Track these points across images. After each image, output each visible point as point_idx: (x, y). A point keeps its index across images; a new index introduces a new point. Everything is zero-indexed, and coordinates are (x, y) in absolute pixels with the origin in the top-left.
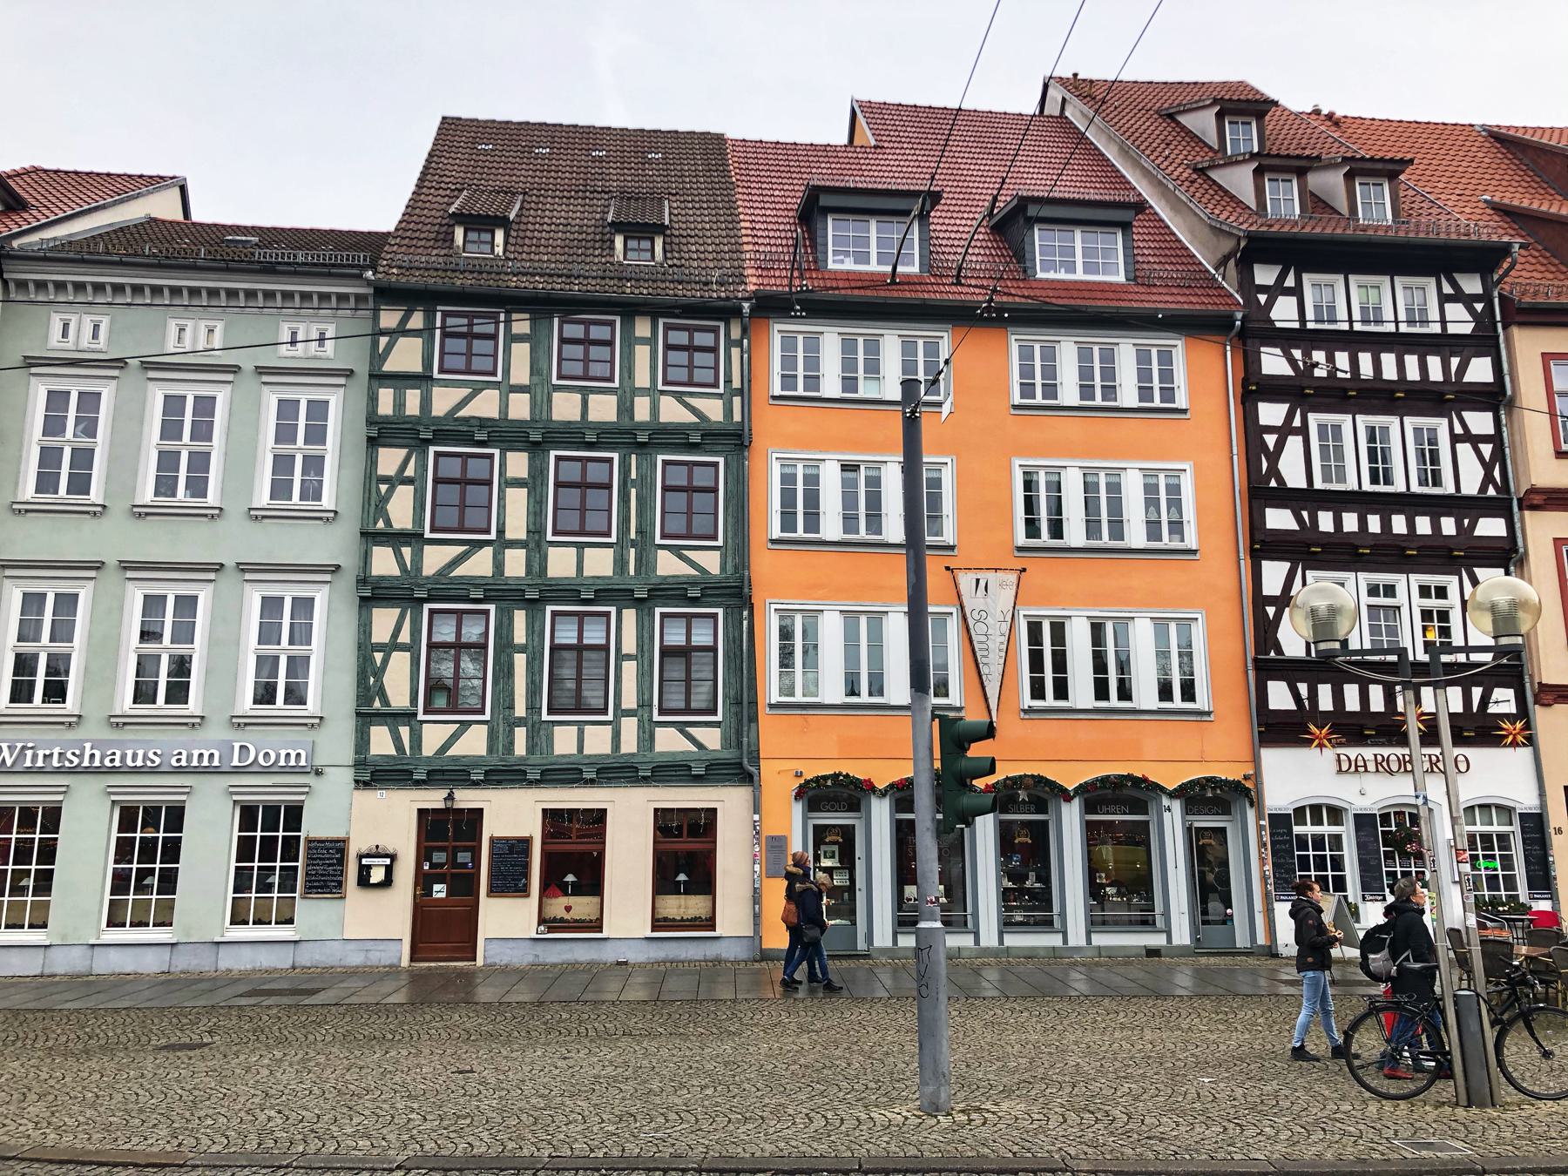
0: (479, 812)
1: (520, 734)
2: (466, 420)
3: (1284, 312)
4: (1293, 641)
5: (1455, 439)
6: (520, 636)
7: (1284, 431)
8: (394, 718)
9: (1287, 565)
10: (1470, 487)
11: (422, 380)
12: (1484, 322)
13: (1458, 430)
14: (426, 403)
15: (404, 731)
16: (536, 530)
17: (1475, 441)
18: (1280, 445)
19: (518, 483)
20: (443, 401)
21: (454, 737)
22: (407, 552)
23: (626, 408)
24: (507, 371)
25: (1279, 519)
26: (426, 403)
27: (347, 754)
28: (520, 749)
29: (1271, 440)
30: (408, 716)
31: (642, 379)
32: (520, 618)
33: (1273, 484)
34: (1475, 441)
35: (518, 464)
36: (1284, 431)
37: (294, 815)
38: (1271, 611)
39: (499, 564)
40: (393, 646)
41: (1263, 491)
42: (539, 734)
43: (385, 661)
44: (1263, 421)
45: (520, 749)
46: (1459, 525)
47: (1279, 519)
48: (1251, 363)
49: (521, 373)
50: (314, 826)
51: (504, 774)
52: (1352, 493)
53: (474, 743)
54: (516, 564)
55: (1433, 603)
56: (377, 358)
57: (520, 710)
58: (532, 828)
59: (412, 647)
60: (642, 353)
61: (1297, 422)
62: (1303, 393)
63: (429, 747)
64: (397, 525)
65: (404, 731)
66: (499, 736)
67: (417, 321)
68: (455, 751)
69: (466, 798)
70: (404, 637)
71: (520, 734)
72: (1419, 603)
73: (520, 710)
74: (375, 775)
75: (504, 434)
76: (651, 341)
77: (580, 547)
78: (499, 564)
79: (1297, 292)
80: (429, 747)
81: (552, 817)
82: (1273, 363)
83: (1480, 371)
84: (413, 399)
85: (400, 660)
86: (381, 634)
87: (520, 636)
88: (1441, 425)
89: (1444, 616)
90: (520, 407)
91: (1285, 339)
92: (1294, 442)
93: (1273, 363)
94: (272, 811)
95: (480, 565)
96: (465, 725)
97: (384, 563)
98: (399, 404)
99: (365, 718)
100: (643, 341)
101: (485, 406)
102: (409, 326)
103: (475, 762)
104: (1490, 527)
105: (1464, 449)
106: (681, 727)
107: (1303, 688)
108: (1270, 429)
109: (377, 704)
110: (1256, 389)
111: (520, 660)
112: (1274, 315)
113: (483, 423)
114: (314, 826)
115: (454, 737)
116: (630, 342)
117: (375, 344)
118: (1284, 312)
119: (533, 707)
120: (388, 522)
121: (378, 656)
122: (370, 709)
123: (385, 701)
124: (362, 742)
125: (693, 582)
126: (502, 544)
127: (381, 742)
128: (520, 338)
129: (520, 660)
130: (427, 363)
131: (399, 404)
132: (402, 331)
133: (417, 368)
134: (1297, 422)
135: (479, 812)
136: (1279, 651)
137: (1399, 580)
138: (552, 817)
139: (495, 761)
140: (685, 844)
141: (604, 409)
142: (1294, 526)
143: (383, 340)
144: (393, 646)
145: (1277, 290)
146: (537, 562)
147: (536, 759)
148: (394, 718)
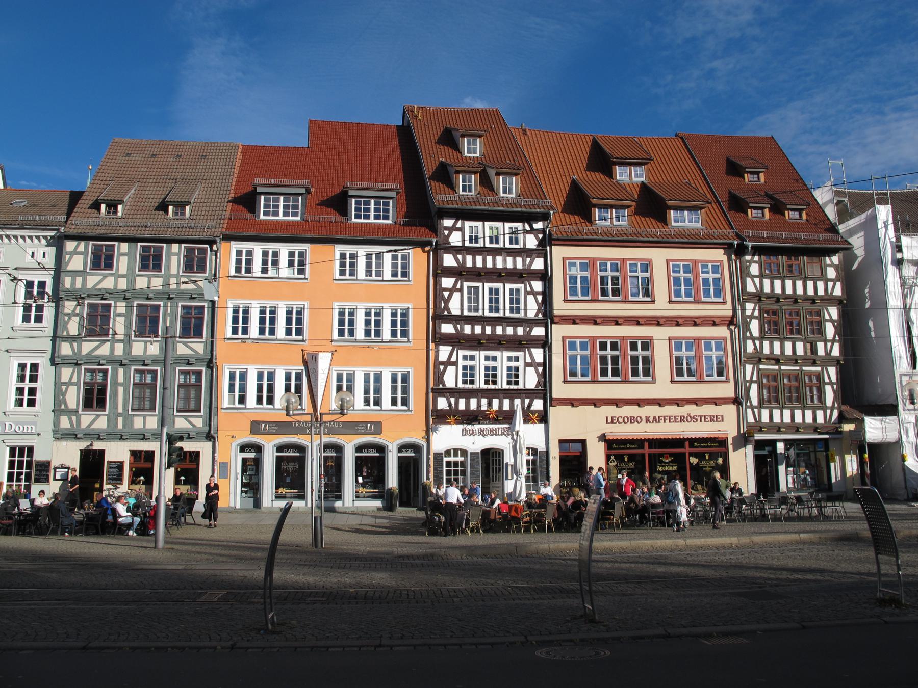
0: (102, 452)
1: (120, 420)
2: (100, 290)
3: (455, 239)
4: (450, 379)
5: (527, 293)
6: (121, 379)
7: (452, 290)
8: (71, 413)
9: (450, 348)
10: (531, 314)
11: (82, 273)
12: (542, 244)
13: (529, 289)
14: (84, 282)
15: (74, 418)
16: (128, 336)
17: (534, 294)
18: (450, 296)
19: (121, 315)
20: (91, 281)
22: (75, 345)
23: (166, 284)
24: (118, 269)
25: (447, 328)
26: (84, 282)
27: (50, 427)
29: (446, 294)
30: (75, 412)
31: (174, 271)
32: (121, 371)
33: (446, 313)
34: (534, 294)
35: (121, 308)
36: (452, 290)
37: (31, 450)
38: (442, 367)
39: (112, 349)
40: (69, 383)
41: (439, 316)
42: (128, 420)
43: (67, 390)
44: (444, 286)
45: (120, 426)
46: (525, 330)
47: (447, 328)
48: (438, 261)
49: (123, 270)
50: (38, 457)
52: (480, 317)
53: (102, 423)
54: (119, 349)
55: (513, 364)
57: (120, 410)
58: (126, 459)
59: (77, 384)
60: (174, 259)
61: (458, 286)
62: (459, 273)
63: (84, 425)
64: (72, 333)
65: (74, 418)
66: (112, 421)
68: (94, 426)
69: (98, 446)
70: (74, 380)
71: (120, 420)
72: (507, 364)
73: (120, 410)
74: (61, 435)
75: (116, 294)
76: (178, 254)
77: (146, 342)
78: (112, 349)
79: (461, 230)
80: (84, 425)
81: (134, 454)
82: (449, 260)
83: (538, 264)
84: (79, 280)
85: (72, 390)
86: (65, 378)
87: (121, 379)
88: (520, 286)
89: (517, 369)
90: (123, 284)
91: (455, 250)
92: (457, 295)
93: (449, 260)
94: (22, 450)
95: (105, 350)
96: (98, 416)
97: (66, 349)
98: (73, 283)
100: (175, 254)
101: (108, 284)
102: (78, 250)
103: (103, 430)
104: (539, 331)
105: (530, 298)
106: (186, 418)
107: (453, 400)
108: (446, 289)
109: (63, 407)
110: (440, 271)
111: (121, 390)
112: (451, 240)
113: (107, 291)
114: (38, 457)
116: (169, 254)
118: (455, 239)
119: (125, 408)
120: (68, 332)
121: (64, 388)
122: (59, 410)
124: (57, 422)
125: (192, 356)
126: (114, 341)
127: (65, 423)
128: (124, 254)
129: (121, 390)
131: (73, 283)
132: (75, 252)
134: (458, 286)
135: (102, 452)
136: (444, 385)
137: (497, 353)
138: (134, 454)
139: (111, 431)
140: (143, 465)
141: (157, 283)
142: (453, 331)
144: (69, 383)
145: (453, 229)
146: (128, 349)
147: (126, 430)
148: (71, 413)
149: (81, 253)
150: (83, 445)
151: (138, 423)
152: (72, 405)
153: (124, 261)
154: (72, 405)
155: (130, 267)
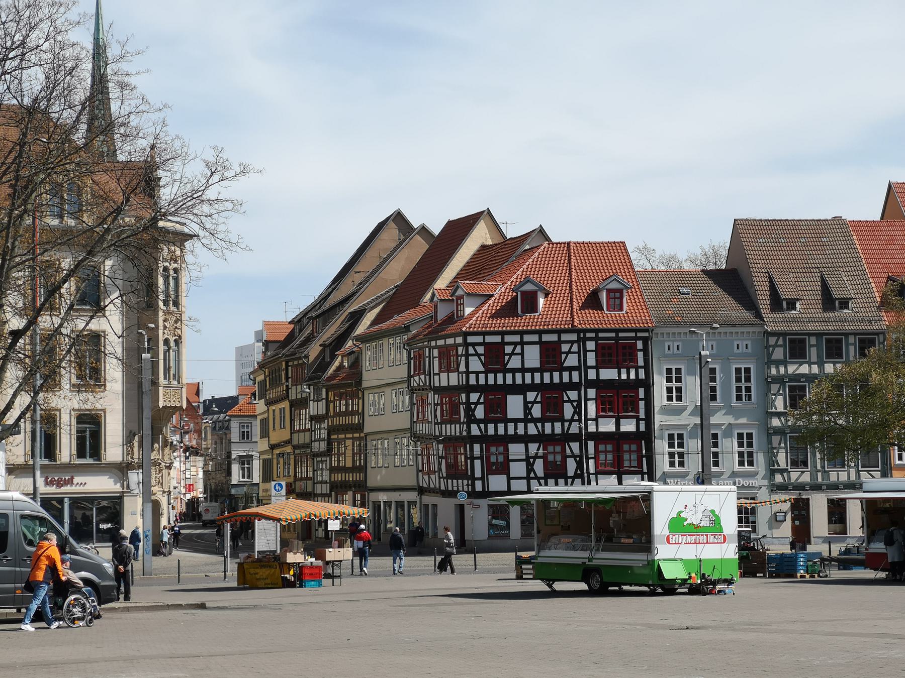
8: (782, 471)
15: (785, 474)
20: (791, 369)
21: (800, 476)
28: (820, 480)
30: (786, 470)
45: (820, 480)
49: (814, 358)
51: (817, 488)
53: (806, 478)
56: (769, 355)
57: (819, 468)
60: (852, 348)
64: (779, 410)
66: (813, 476)
67: (781, 342)
71: (819, 474)
76: (854, 344)
86: (775, 444)
90: (815, 369)
99: (772, 472)
100: (852, 344)
103: (807, 484)
109: (776, 467)
115: (800, 476)
116: (847, 345)
117: (768, 350)
123: (779, 465)
130: (785, 357)
133: (782, 357)
139: (813, 483)
143: (771, 349)
147: (825, 482)
148: (782, 471)
149: (780, 346)
150: (794, 495)
151: (833, 477)
152: (783, 465)
153: (814, 351)
154: (783, 465)
155: (819, 356)
